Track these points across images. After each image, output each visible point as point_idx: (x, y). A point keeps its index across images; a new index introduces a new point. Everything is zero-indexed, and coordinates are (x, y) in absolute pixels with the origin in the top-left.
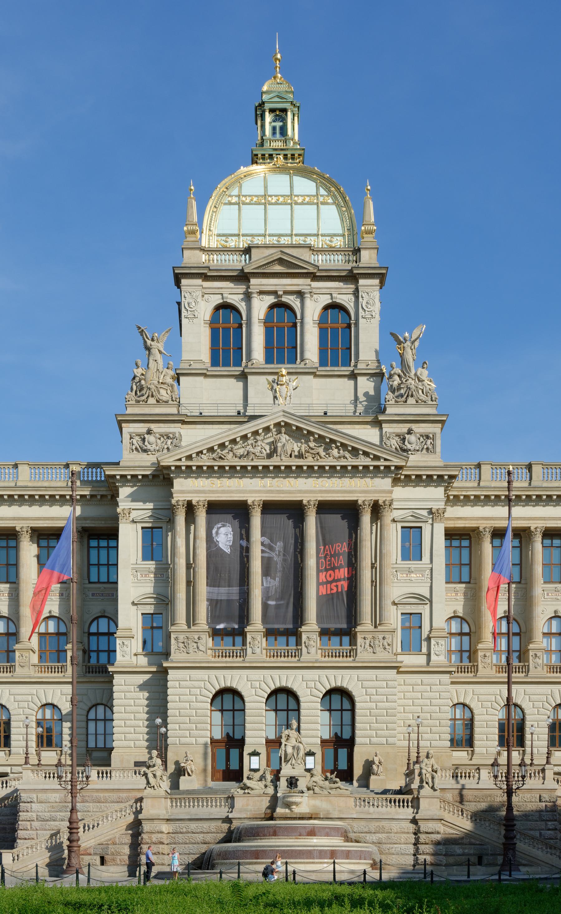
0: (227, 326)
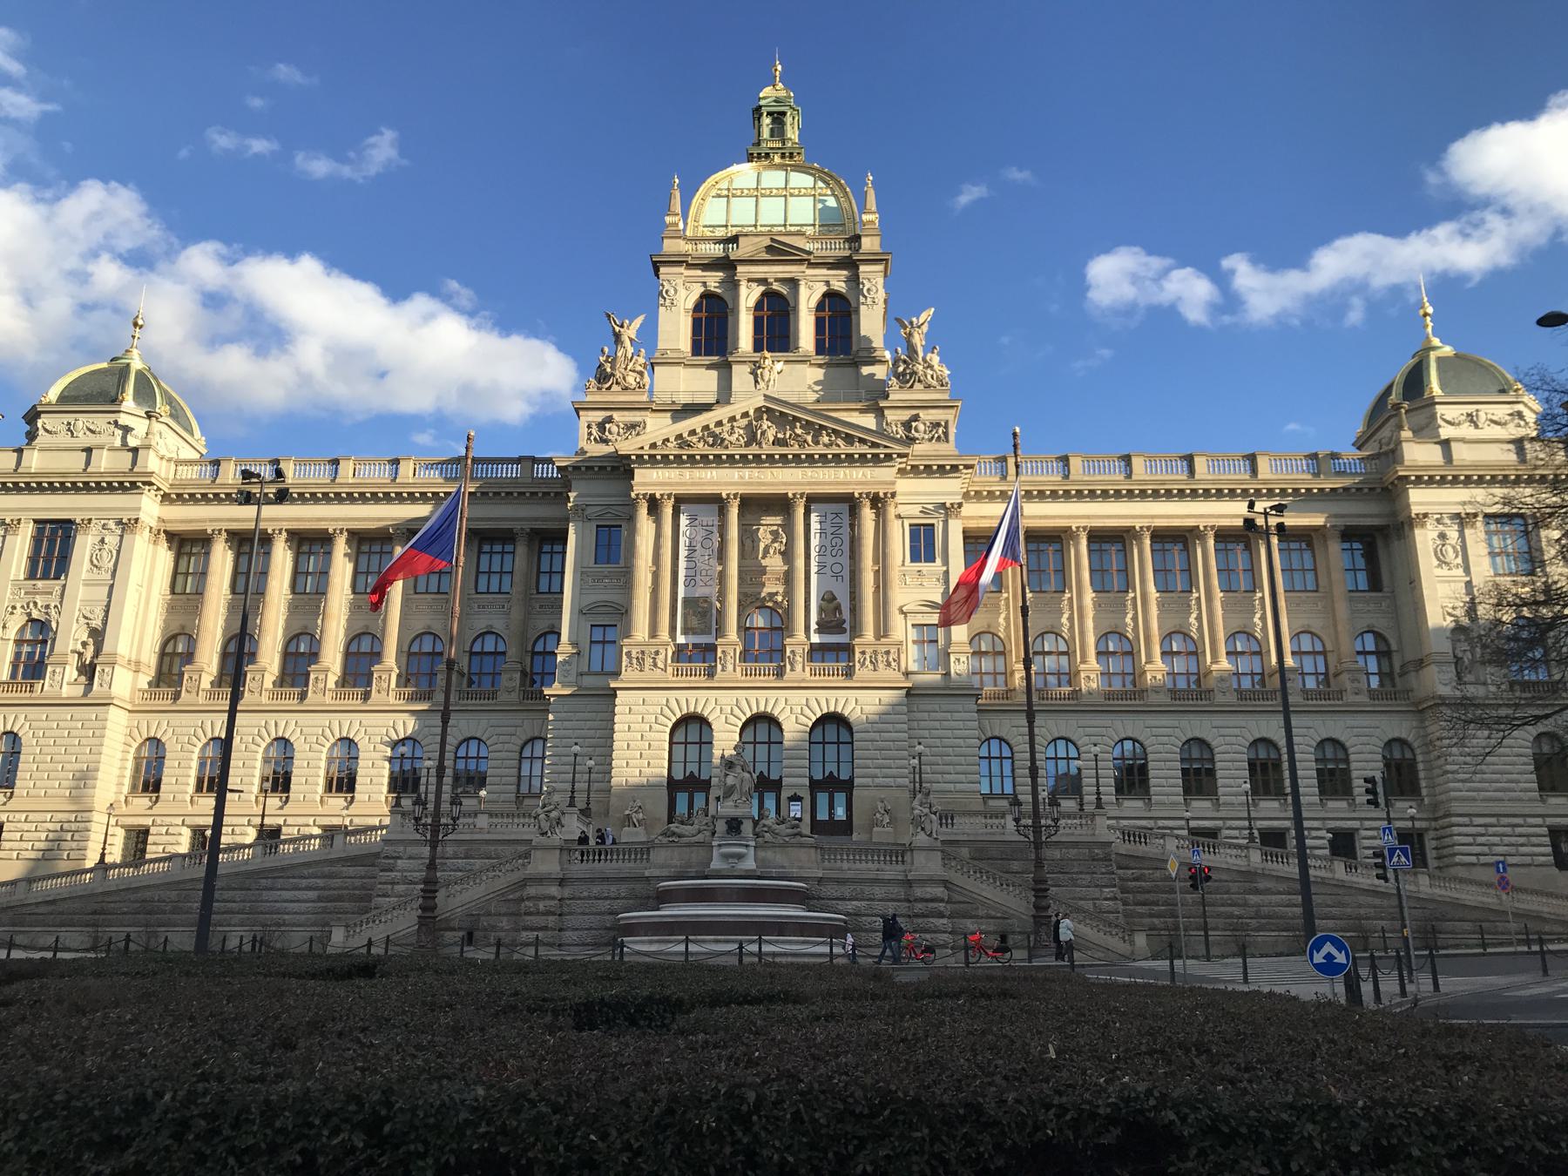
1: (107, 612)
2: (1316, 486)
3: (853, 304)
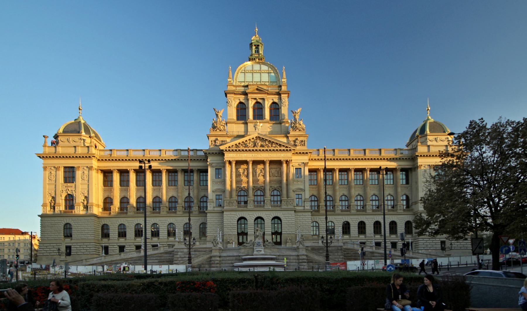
0: (242, 109)
2: (396, 157)
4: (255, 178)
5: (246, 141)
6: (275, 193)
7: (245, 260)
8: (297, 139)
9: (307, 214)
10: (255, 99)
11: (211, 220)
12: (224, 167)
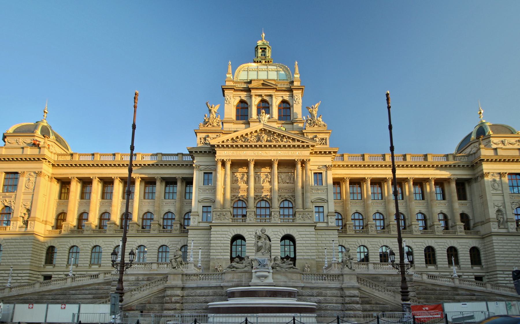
1: (32, 203)
2: (448, 163)
3: (291, 104)
4: (257, 185)
5: (247, 134)
6: (286, 204)
7: (232, 295)
8: (316, 137)
9: (331, 232)
10: (261, 96)
11: (194, 240)
12: (215, 170)
